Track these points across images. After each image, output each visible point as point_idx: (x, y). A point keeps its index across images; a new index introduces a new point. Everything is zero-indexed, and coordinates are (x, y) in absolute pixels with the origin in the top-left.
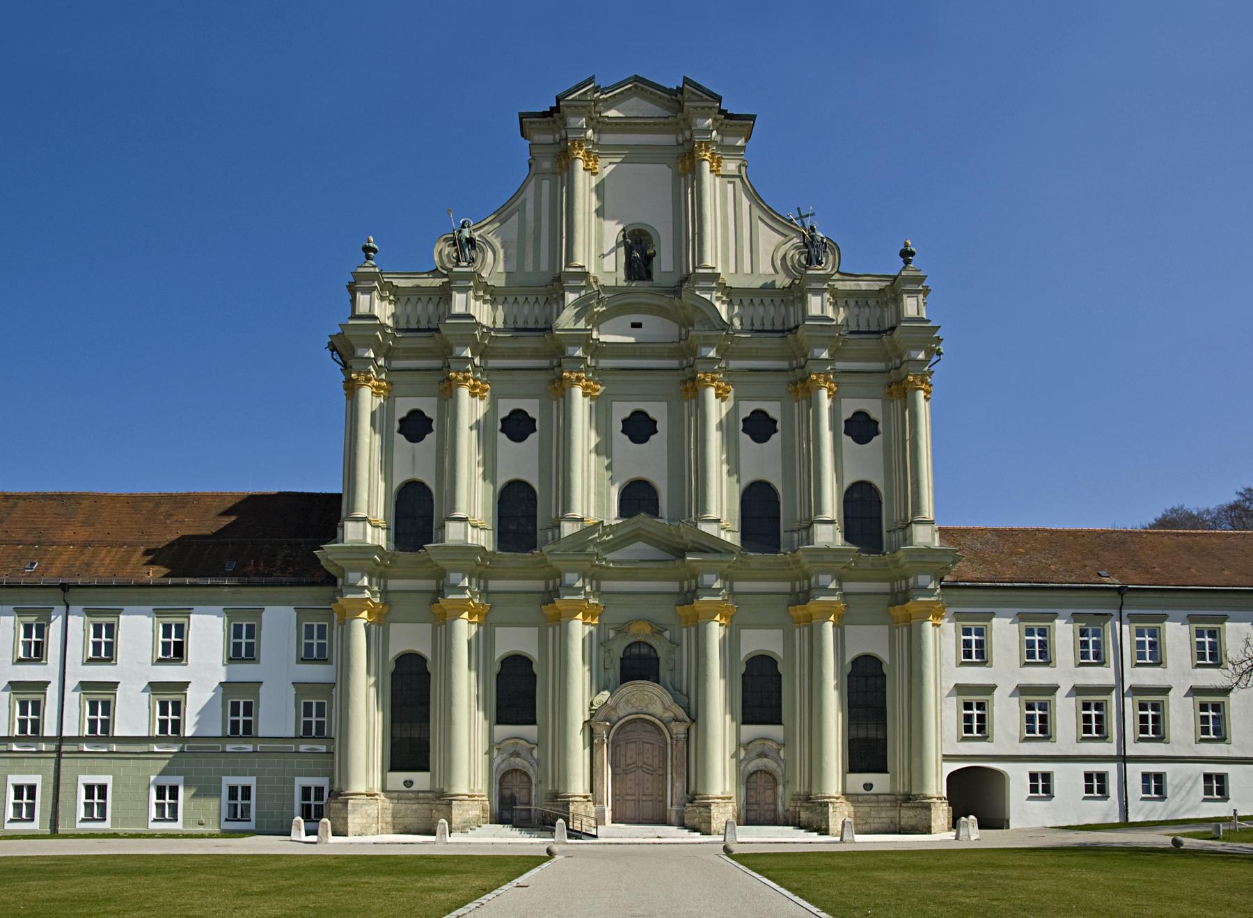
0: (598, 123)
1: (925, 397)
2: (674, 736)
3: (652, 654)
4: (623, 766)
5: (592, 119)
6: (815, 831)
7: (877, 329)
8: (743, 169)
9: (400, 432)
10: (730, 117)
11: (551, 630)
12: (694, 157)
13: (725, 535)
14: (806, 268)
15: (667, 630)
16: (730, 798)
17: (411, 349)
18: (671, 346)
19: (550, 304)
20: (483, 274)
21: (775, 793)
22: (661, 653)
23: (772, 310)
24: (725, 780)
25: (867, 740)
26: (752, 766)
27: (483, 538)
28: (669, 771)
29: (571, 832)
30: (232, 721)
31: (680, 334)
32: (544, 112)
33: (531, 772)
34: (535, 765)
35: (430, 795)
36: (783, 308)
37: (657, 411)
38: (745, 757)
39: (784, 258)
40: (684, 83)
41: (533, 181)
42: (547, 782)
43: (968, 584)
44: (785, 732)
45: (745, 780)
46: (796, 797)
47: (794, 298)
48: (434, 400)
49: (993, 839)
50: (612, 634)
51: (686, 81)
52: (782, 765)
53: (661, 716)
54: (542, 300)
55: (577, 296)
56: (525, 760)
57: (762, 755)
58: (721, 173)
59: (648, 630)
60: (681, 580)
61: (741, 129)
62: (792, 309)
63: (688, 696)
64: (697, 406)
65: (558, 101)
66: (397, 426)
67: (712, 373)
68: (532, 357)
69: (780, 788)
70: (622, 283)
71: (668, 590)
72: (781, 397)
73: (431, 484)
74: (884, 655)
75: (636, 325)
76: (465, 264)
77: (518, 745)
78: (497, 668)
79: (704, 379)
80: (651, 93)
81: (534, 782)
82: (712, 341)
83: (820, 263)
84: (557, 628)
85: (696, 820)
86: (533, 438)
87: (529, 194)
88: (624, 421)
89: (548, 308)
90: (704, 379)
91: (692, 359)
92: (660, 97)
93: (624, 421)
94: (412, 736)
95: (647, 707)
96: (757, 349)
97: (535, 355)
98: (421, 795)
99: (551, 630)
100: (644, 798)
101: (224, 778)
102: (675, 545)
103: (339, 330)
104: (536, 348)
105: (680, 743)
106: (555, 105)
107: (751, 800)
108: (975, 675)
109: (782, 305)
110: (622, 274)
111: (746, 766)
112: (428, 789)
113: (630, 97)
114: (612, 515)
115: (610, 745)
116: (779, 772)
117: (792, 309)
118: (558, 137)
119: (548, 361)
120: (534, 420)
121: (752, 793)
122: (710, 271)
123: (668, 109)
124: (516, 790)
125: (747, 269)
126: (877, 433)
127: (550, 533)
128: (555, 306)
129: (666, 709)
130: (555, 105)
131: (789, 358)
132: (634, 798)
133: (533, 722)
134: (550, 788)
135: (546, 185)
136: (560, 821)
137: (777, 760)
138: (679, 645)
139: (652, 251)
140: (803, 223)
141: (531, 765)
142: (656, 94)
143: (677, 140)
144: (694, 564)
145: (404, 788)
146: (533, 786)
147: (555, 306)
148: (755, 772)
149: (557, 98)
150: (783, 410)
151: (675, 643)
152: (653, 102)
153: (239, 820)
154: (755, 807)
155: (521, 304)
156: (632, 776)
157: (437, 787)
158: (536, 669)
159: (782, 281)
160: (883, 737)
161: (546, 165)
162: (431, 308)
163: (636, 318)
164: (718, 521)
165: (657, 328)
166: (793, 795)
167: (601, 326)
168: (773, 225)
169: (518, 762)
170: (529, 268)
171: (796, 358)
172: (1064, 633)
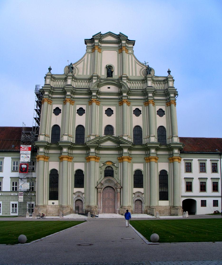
0: (102, 41)
1: (175, 106)
3: (112, 169)
4: (105, 198)
5: (100, 41)
6: (151, 215)
7: (163, 89)
9: (53, 113)
10: (130, 41)
11: (87, 163)
12: (122, 49)
13: (129, 139)
14: (147, 75)
15: (115, 164)
16: (131, 207)
19: (89, 82)
20: (75, 75)
21: (142, 206)
22: (114, 169)
23: (139, 85)
24: (129, 202)
25: (163, 192)
26: (136, 199)
27: (72, 140)
28: (116, 200)
29: (92, 215)
30: (13, 187)
32: (90, 39)
33: (82, 200)
36: (142, 85)
37: (113, 108)
38: (134, 196)
40: (120, 33)
41: (87, 54)
42: (86, 203)
43: (186, 152)
44: (144, 190)
45: (134, 202)
47: (145, 82)
48: (62, 105)
49: (192, 217)
50: (102, 165)
51: (120, 33)
52: (143, 198)
54: (88, 81)
55: (96, 81)
57: (138, 196)
58: (128, 53)
61: (132, 43)
62: (144, 84)
63: (121, 181)
64: (123, 107)
65: (93, 36)
66: (53, 111)
69: (143, 204)
70: (106, 78)
73: (60, 125)
74: (167, 170)
76: (70, 73)
78: (75, 173)
80: (113, 35)
83: (150, 74)
84: (89, 163)
85: (122, 212)
86: (84, 115)
87: (86, 57)
88: (106, 111)
89: (89, 83)
91: (121, 96)
92: (115, 36)
93: (106, 111)
97: (85, 94)
99: (87, 163)
100: (110, 207)
103: (42, 88)
105: (118, 193)
106: (92, 38)
107: (136, 207)
108: (188, 175)
109: (142, 83)
110: (106, 76)
111: (135, 199)
113: (108, 36)
114: (103, 134)
115: (102, 193)
116: (142, 200)
117: (144, 84)
118: (93, 44)
119: (88, 96)
120: (85, 110)
121: (136, 205)
122: (125, 75)
123: (117, 39)
124: (79, 205)
125: (134, 75)
126: (164, 114)
127: (88, 139)
128: (90, 83)
130: (92, 38)
132: (107, 207)
133: (83, 187)
135: (89, 55)
136: (89, 213)
139: (113, 71)
140: (146, 65)
142: (114, 36)
143: (118, 46)
144: (121, 147)
145: (52, 204)
147: (90, 83)
148: (137, 200)
149: (93, 36)
152: (114, 37)
154: (137, 209)
155: (88, 82)
156: (107, 201)
160: (167, 191)
161: (90, 50)
162: (62, 83)
163: (109, 86)
164: (127, 136)
165: (113, 89)
167: (101, 88)
169: (79, 198)
170: (85, 74)
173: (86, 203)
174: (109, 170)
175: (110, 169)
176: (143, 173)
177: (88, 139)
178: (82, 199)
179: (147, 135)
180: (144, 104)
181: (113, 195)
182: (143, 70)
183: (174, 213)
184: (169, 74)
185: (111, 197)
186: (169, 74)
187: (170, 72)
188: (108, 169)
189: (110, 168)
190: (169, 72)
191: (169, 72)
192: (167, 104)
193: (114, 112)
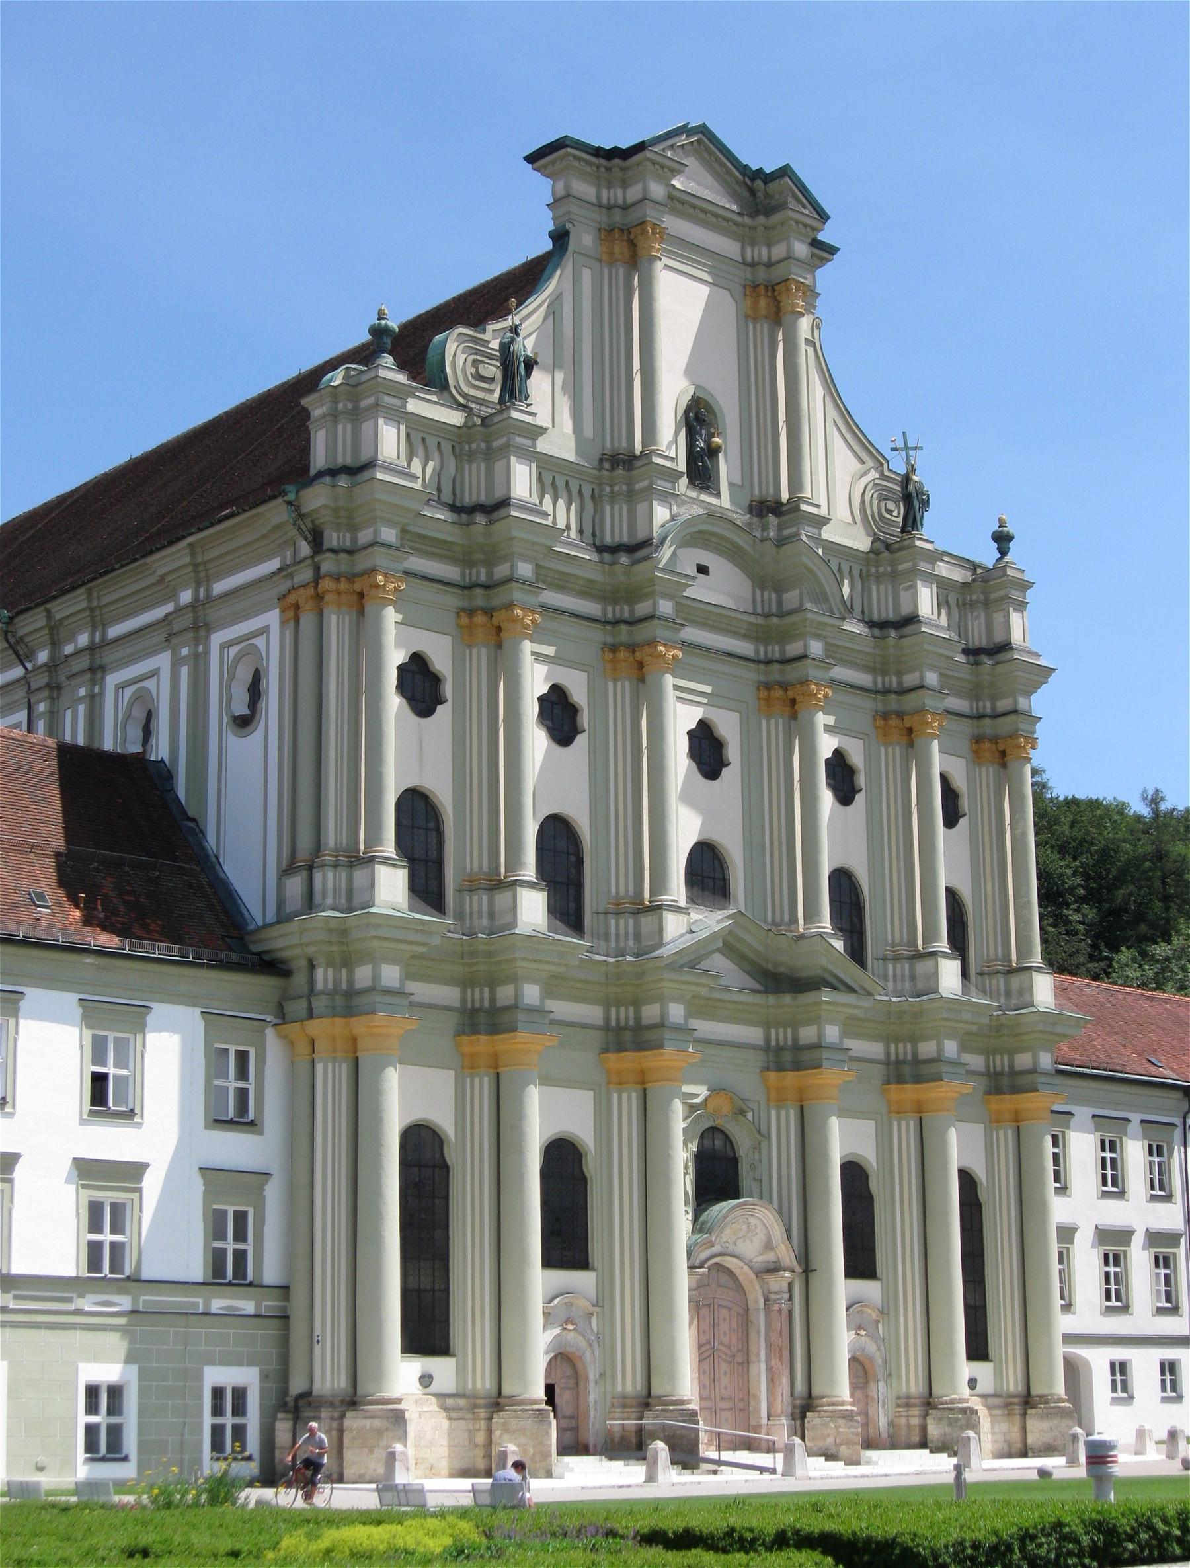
2: (772, 1296)
8: (816, 332)
11: (615, 1096)
17: (425, 537)
18: (752, 619)
22: (743, 1146)
31: (754, 601)
34: (595, 1344)
35: (462, 1402)
39: (863, 502)
46: (906, 1402)
53: (751, 1261)
56: (583, 1336)
59: (726, 1109)
60: (767, 1025)
67: (826, 687)
68: (583, 594)
71: (739, 1040)
72: (866, 734)
75: (703, 570)
77: (574, 1308)
79: (816, 694)
81: (592, 1375)
82: (825, 633)
90: (816, 694)
94: (422, 1286)
95: (735, 1243)
96: (846, 648)
97: (587, 591)
98: (450, 1402)
101: (81, 1366)
102: (770, 967)
104: (591, 581)
112: (453, 1390)
129: (768, 1246)
131: (872, 670)
134: (620, 1388)
137: (873, 1336)
138: (769, 1137)
141: (591, 1345)
146: (592, 1384)
150: (867, 756)
151: (762, 1135)
153: (103, 1459)
157: (470, 1386)
158: (591, 1166)
159: (861, 542)
163: (705, 557)
166: (899, 1398)
168: (848, 436)
171: (884, 673)
172: (1135, 1152)
173: (609, 1380)
174: (714, 1149)
175: (719, 1143)
176: (873, 1185)
177: (613, 922)
178: (582, 1343)
179: (889, 938)
180: (877, 728)
181: (734, 1325)
182: (864, 481)
183: (1047, 1438)
184: (1003, 552)
185: (726, 1340)
186: (1003, 552)
187: (1009, 538)
188: (711, 1141)
189: (721, 1136)
190: (1002, 540)
191: (1002, 540)
192: (976, 752)
193: (733, 753)
